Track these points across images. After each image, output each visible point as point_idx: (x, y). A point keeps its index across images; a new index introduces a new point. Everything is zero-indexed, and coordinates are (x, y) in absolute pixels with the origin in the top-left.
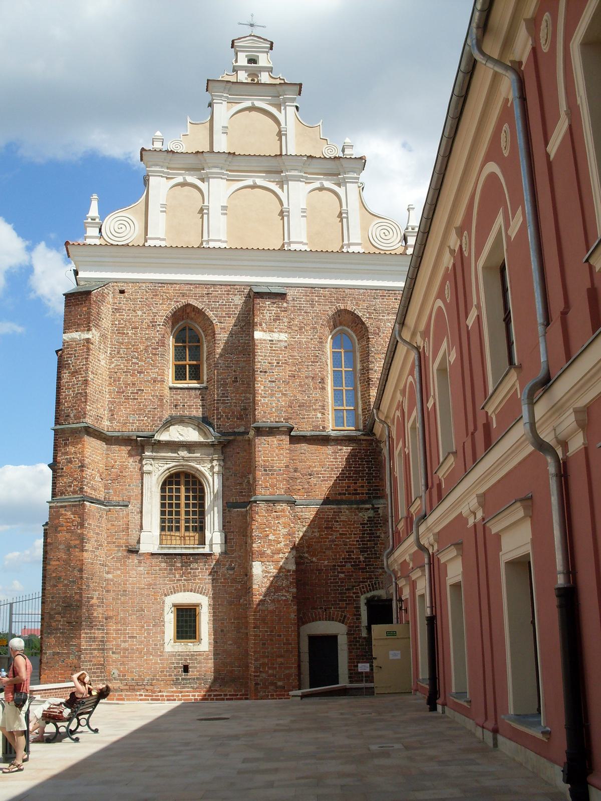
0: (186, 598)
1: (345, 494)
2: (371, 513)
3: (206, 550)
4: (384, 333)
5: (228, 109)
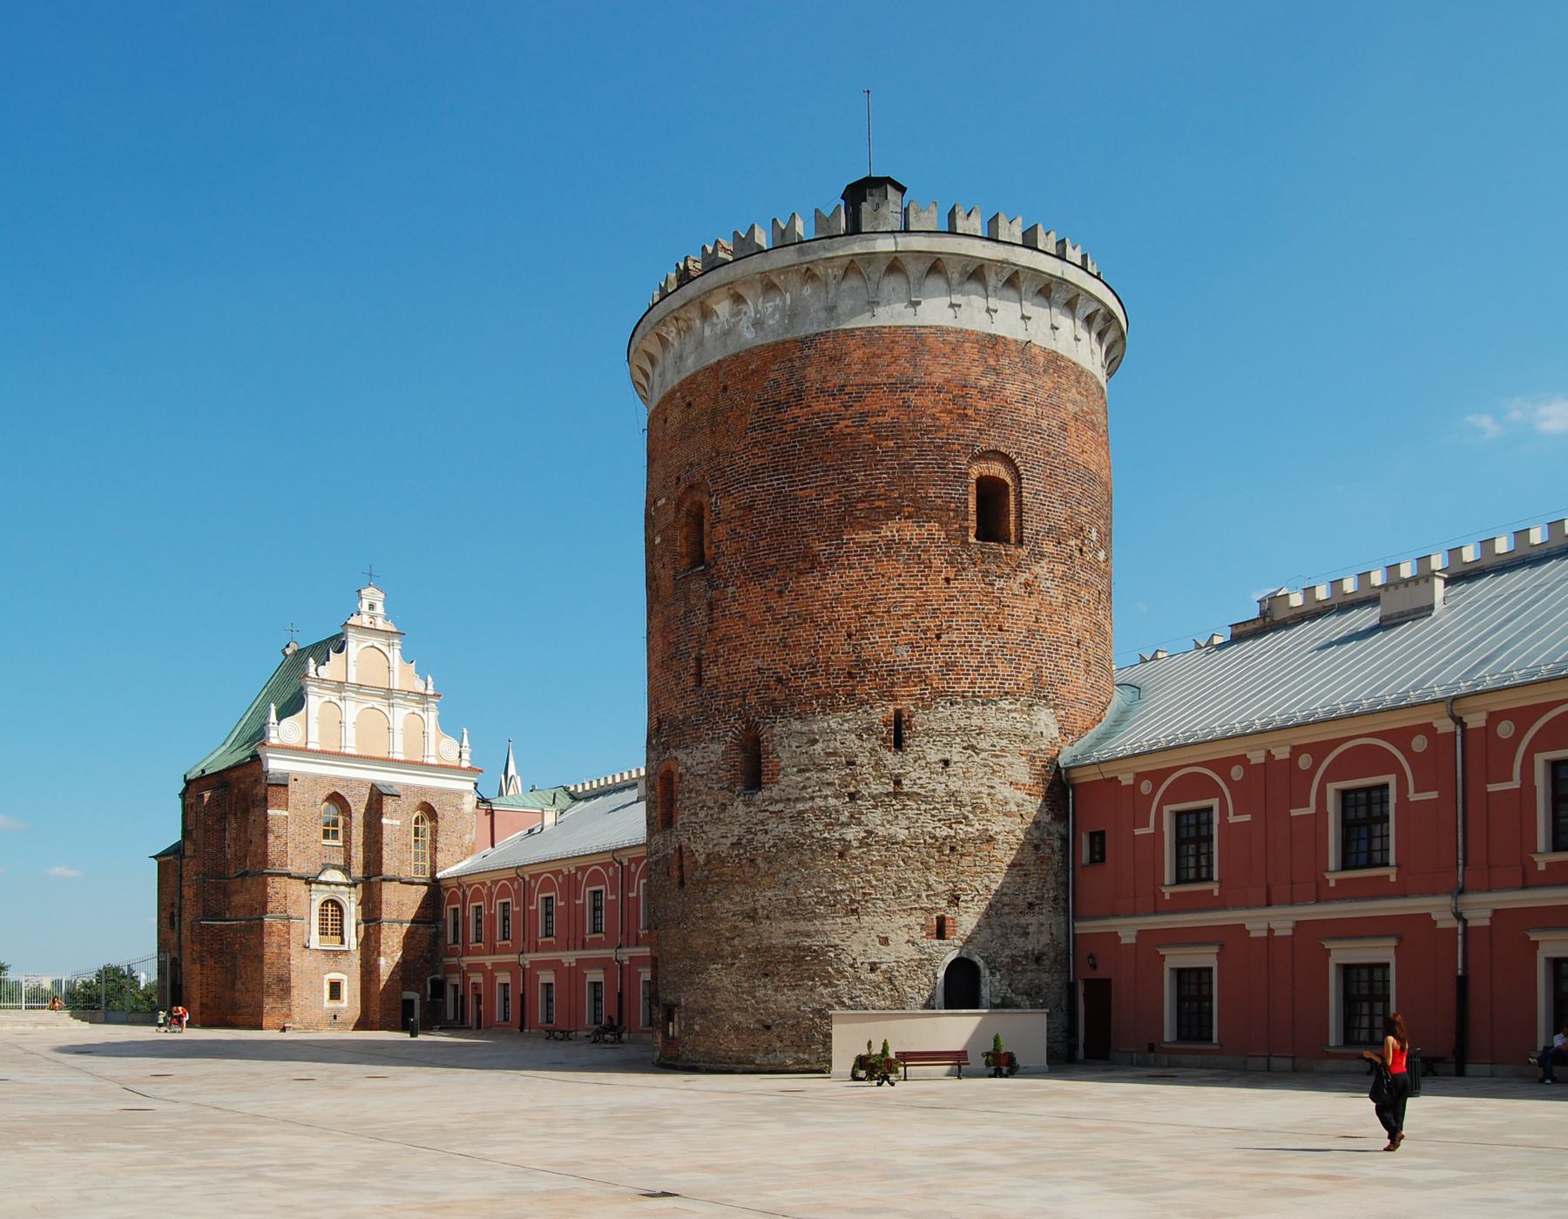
0: (335, 976)
3: (345, 948)
5: (357, 646)
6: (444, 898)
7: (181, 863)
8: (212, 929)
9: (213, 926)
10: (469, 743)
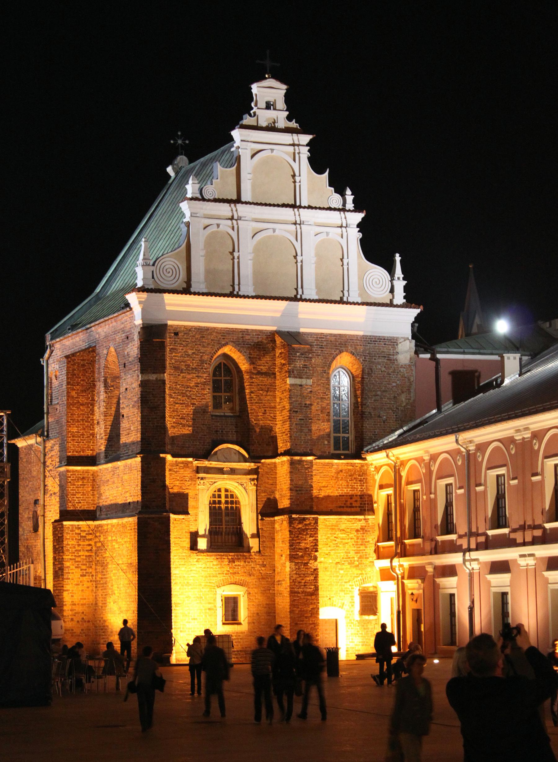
1: (343, 507)
2: (363, 523)
4: (375, 374)
6: (375, 481)
7: (45, 448)
8: (77, 531)
9: (79, 528)
10: (403, 272)
